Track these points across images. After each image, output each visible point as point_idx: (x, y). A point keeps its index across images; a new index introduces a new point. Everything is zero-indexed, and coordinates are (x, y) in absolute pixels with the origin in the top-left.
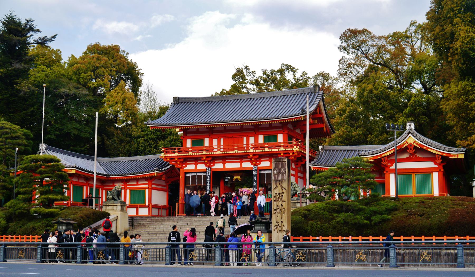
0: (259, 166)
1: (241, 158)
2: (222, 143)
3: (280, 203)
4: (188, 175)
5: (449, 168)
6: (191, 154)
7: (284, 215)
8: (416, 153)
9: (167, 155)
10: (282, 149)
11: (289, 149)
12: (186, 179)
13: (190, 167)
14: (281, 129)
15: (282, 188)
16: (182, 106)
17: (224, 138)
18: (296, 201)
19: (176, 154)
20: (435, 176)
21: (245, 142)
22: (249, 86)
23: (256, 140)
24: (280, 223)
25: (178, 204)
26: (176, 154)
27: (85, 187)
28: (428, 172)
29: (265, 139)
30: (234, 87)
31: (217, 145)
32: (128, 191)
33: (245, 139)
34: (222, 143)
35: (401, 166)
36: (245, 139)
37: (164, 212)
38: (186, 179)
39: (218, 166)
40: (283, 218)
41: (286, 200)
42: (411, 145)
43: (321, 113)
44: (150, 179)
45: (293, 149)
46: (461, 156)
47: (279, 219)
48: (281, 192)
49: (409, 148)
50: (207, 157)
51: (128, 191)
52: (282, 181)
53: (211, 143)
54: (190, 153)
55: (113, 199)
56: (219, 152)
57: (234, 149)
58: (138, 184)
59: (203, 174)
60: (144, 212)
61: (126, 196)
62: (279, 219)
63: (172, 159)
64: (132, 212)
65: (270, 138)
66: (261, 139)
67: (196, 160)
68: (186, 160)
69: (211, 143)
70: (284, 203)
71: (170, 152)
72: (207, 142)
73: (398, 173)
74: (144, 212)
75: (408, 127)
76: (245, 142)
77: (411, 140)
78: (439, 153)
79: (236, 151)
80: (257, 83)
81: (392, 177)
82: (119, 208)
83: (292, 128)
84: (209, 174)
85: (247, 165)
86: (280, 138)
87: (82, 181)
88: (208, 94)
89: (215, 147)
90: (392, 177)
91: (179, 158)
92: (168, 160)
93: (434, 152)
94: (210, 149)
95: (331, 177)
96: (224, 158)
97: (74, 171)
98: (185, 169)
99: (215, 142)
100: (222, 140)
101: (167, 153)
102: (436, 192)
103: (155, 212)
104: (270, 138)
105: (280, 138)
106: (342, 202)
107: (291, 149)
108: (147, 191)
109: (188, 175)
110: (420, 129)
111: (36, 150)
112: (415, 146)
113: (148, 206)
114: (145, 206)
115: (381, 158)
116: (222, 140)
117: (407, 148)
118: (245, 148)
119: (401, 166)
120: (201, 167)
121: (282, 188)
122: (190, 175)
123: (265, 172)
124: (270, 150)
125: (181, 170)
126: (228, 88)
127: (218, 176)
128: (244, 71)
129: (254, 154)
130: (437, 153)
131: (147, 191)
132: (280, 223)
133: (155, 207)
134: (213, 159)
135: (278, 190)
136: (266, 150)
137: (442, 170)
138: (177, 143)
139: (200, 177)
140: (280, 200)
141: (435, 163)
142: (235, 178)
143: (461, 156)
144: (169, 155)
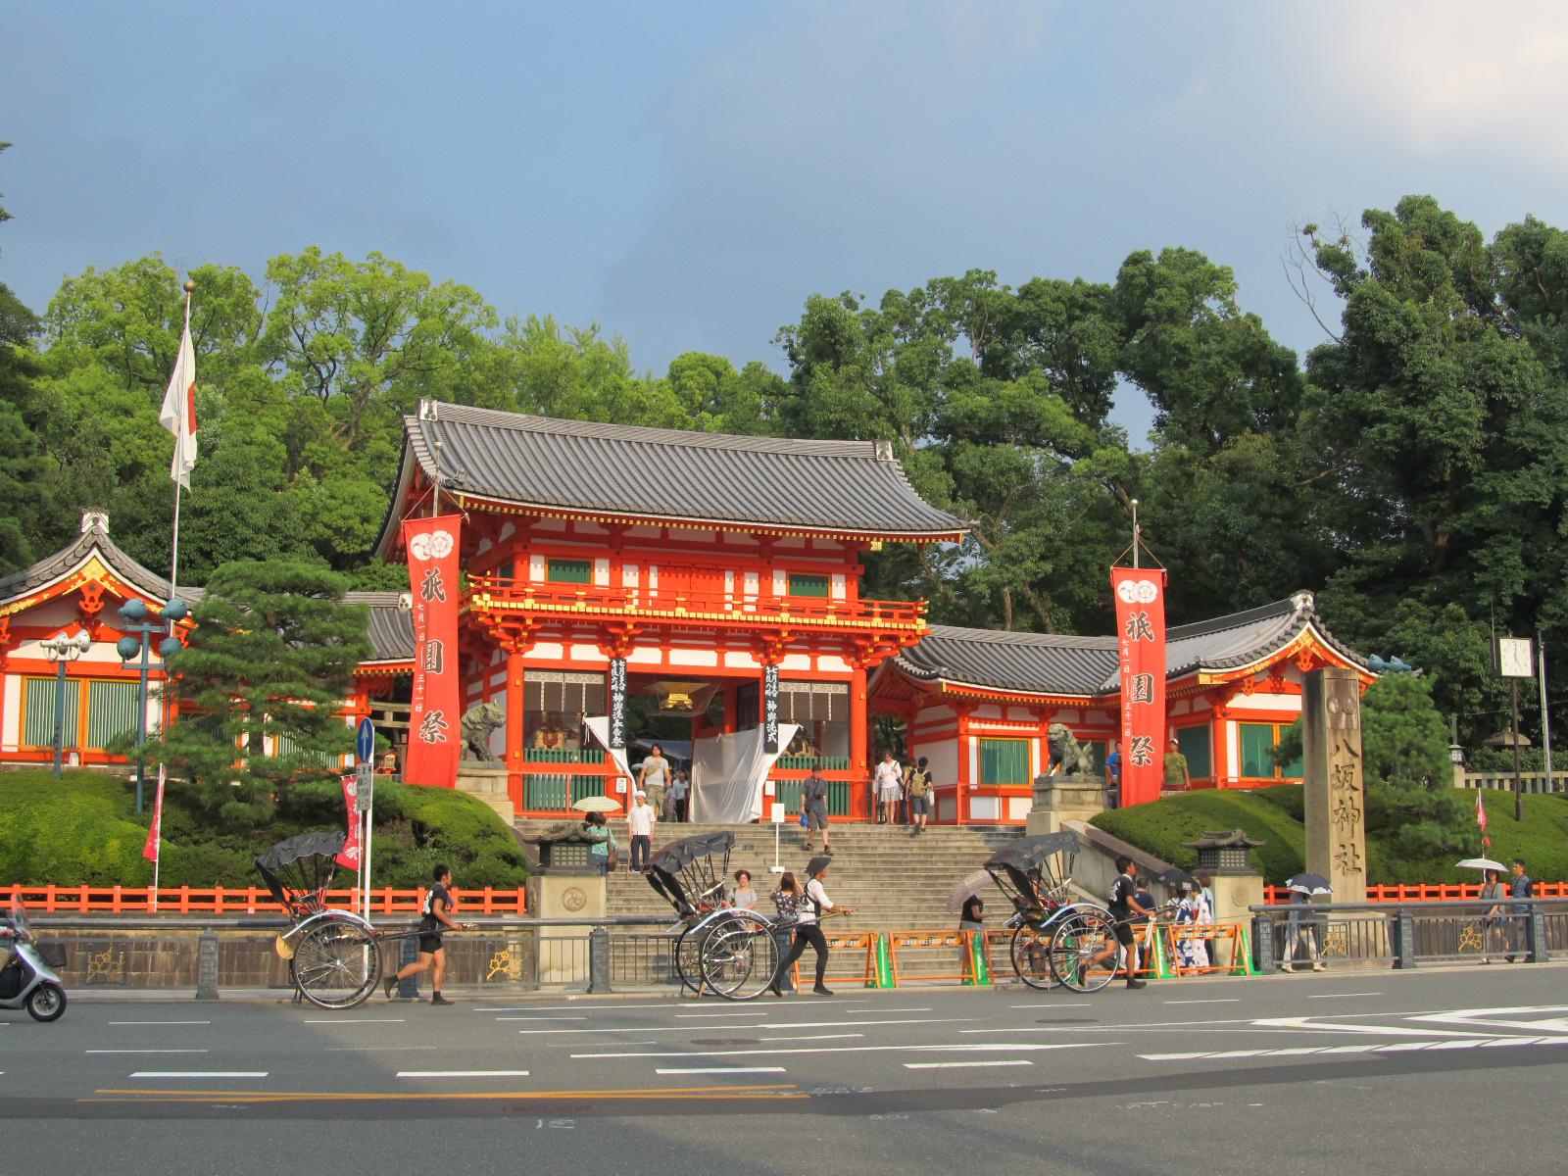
0: (782, 666)
1: (721, 637)
4: (531, 677)
6: (686, 615)
9: (498, 604)
11: (901, 626)
13: (547, 651)
14: (841, 561)
17: (665, 568)
18: (1085, 786)
24: (1349, 849)
31: (637, 588)
38: (531, 689)
39: (646, 656)
41: (1361, 787)
42: (1306, 650)
45: (914, 627)
48: (1348, 762)
49: (1302, 657)
56: (736, 615)
59: (584, 680)
67: (566, 630)
70: (1355, 793)
71: (507, 595)
72: (601, 576)
73: (1247, 719)
81: (1231, 729)
85: (741, 661)
86: (839, 590)
89: (747, 599)
90: (1231, 729)
92: (498, 620)
94: (618, 596)
96: (666, 634)
98: (528, 655)
99: (630, 578)
101: (494, 594)
105: (839, 590)
107: (908, 627)
109: (531, 677)
112: (1314, 656)
115: (1240, 680)
117: (1296, 658)
118: (728, 607)
120: (587, 653)
122: (544, 678)
123: (792, 688)
124: (693, 615)
140: (1346, 785)
142: (673, 699)
144: (505, 605)
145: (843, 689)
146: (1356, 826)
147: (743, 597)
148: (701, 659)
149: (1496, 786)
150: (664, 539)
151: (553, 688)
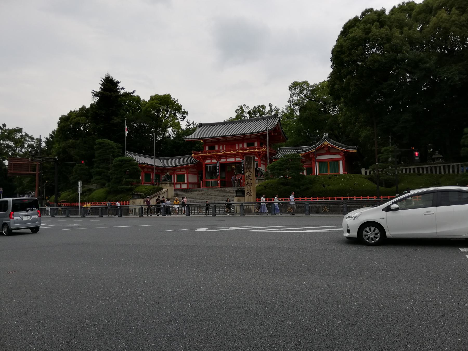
1: (235, 156)
2: (225, 148)
5: (348, 158)
8: (329, 150)
10: (256, 150)
12: (206, 168)
13: (208, 161)
15: (250, 172)
16: (203, 128)
17: (226, 145)
19: (200, 154)
20: (341, 163)
21: (237, 147)
22: (245, 115)
23: (243, 145)
24: (249, 192)
26: (200, 154)
28: (337, 161)
29: (248, 146)
30: (236, 116)
32: (176, 175)
33: (237, 145)
34: (225, 148)
35: (319, 158)
36: (237, 145)
37: (196, 186)
38: (206, 168)
39: (223, 160)
43: (279, 129)
44: (187, 168)
46: (355, 151)
50: (217, 155)
51: (176, 175)
52: (250, 168)
53: (219, 148)
54: (208, 154)
55: (165, 180)
56: (223, 153)
57: (231, 151)
60: (184, 186)
61: (175, 178)
63: (198, 157)
64: (178, 186)
65: (251, 145)
66: (245, 146)
67: (211, 158)
68: (205, 158)
69: (219, 148)
72: (216, 148)
74: (184, 186)
76: (237, 147)
77: (326, 143)
79: (232, 152)
80: (249, 113)
82: (168, 185)
83: (260, 137)
84: (218, 165)
85: (238, 159)
86: (256, 144)
88: (222, 121)
91: (202, 156)
95: (276, 166)
96: (226, 156)
97: (144, 166)
100: (225, 146)
102: (341, 171)
103: (191, 186)
104: (251, 145)
108: (186, 175)
110: (331, 136)
111: (123, 154)
113: (187, 183)
114: (185, 183)
116: (225, 146)
119: (319, 158)
120: (214, 161)
121: (250, 172)
122: (209, 165)
126: (234, 116)
127: (224, 166)
128: (243, 107)
129: (242, 153)
131: (186, 175)
132: (249, 192)
133: (190, 183)
134: (219, 157)
135: (247, 174)
136: (248, 151)
138: (201, 149)
141: (341, 156)
143: (355, 151)
147: (241, 148)
148: (232, 160)
150: (226, 140)
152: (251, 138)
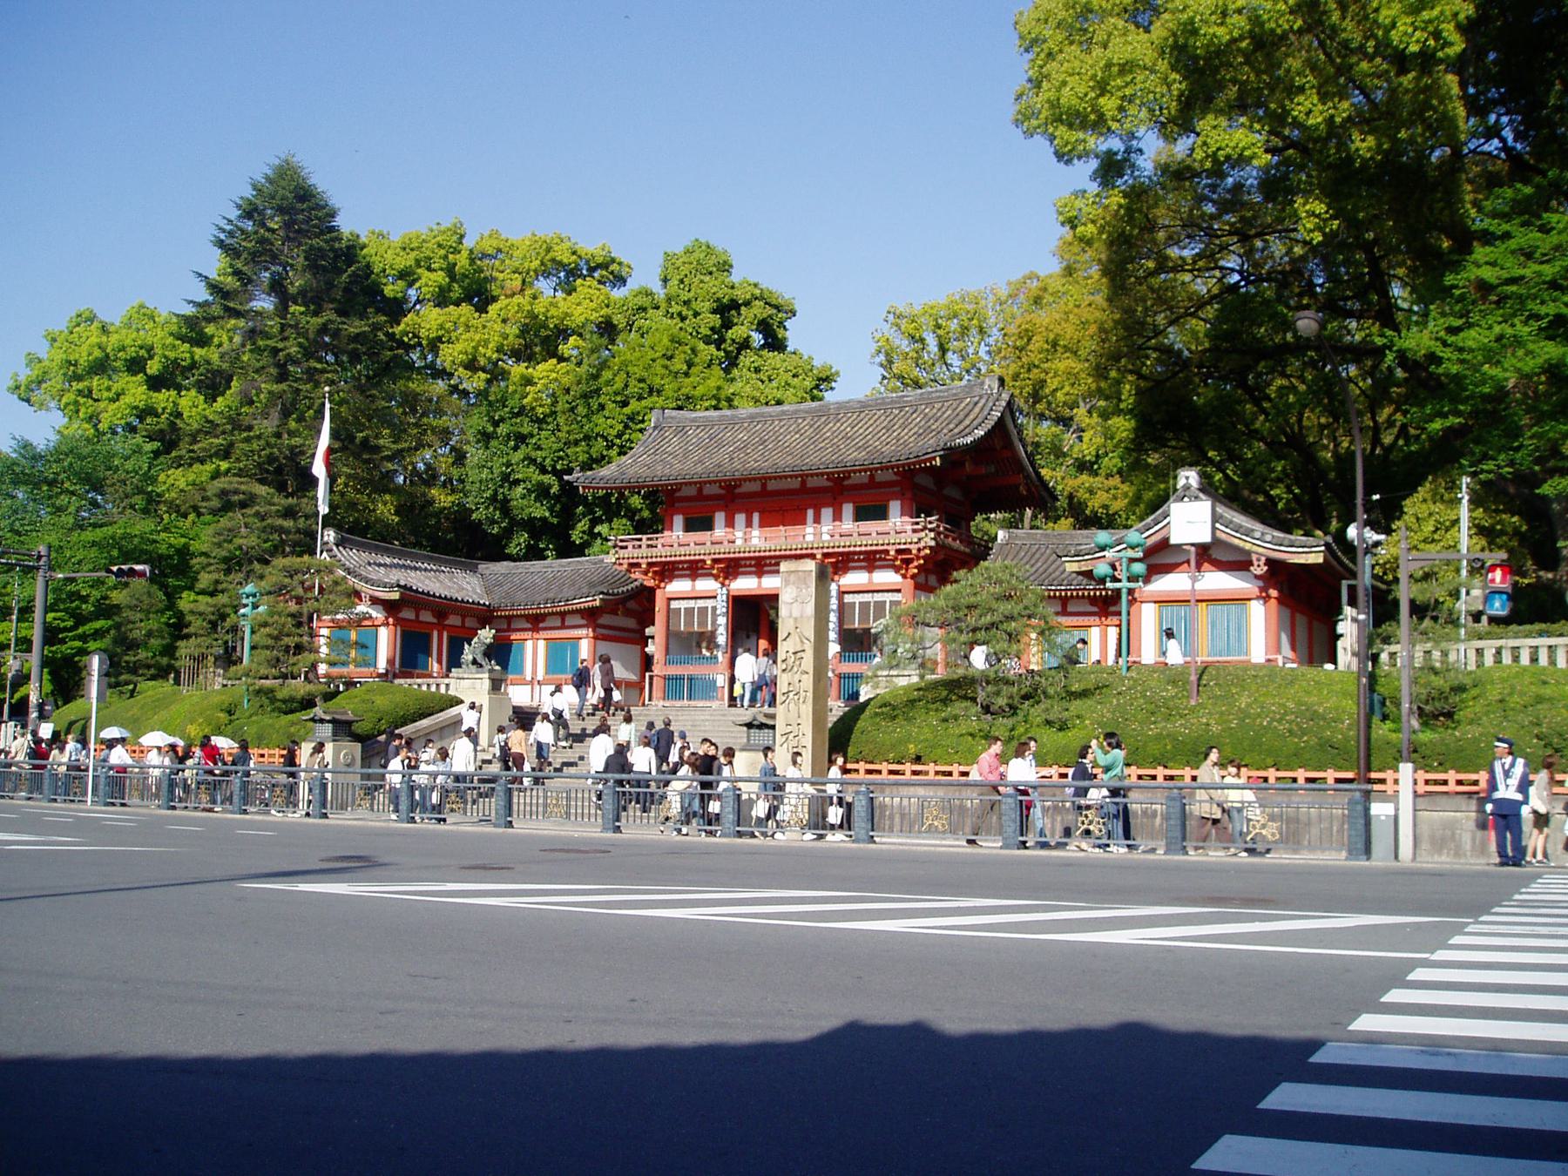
3: (797, 677)
4: (674, 605)
7: (803, 707)
13: (679, 586)
25: (651, 678)
27: (435, 634)
39: (745, 584)
40: (803, 715)
47: (793, 719)
58: (563, 627)
62: (793, 719)
68: (667, 571)
75: (1181, 482)
78: (1261, 550)
82: (487, 684)
84: (721, 605)
87: (427, 617)
93: (1248, 546)
97: (396, 596)
102: (1258, 654)
106: (135, 679)
109: (674, 605)
120: (706, 585)
122: (683, 605)
125: (658, 592)
130: (1255, 548)
137: (1274, 593)
139: (703, 611)
143: (1316, 558)
145: (897, 597)
146: (803, 707)
149: (1507, 659)
151: (689, 611)
152: (872, 483)
